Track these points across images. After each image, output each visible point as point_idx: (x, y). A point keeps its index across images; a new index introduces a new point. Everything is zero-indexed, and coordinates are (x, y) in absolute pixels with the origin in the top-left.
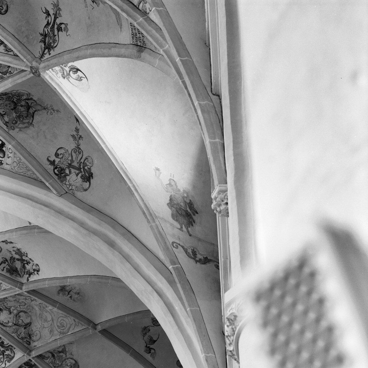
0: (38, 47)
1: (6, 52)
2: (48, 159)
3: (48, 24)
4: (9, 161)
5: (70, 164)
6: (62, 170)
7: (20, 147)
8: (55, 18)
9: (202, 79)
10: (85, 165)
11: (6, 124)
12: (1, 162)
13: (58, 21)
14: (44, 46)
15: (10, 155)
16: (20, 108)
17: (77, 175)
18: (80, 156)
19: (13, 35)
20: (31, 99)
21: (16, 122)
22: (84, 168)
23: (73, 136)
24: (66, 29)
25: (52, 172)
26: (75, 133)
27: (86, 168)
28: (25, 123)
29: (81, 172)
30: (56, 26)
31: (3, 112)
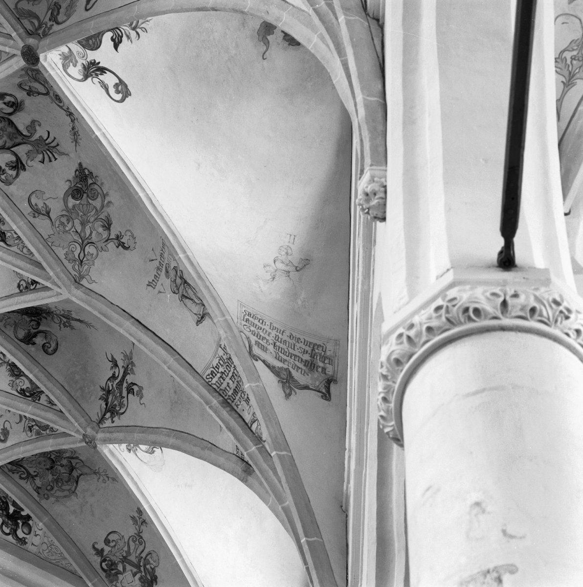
0: (96, 407)
1: (49, 405)
2: (94, 547)
3: (114, 377)
4: (37, 540)
5: (125, 558)
6: (112, 565)
7: (55, 526)
8: (125, 374)
9: (335, 574)
10: (147, 562)
11: (38, 489)
12: (25, 540)
13: (130, 378)
14: (105, 407)
15: (38, 532)
16: (60, 468)
17: (134, 575)
18: (141, 548)
19: (62, 385)
20: (77, 458)
21: (52, 488)
22: (145, 566)
23: (133, 518)
24: (140, 394)
25: (98, 567)
26: (136, 515)
27: (148, 567)
28: (64, 491)
29: (140, 571)
30: (125, 385)
31: (35, 472)
